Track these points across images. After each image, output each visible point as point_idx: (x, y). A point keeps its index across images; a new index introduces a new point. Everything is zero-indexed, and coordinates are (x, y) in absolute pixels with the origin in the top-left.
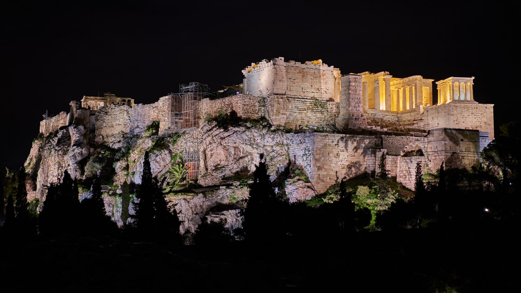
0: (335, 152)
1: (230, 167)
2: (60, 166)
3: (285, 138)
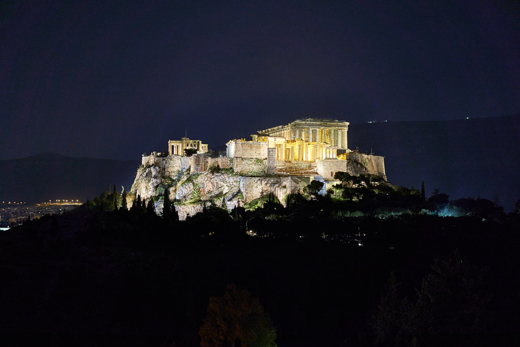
0: (256, 186)
1: (215, 192)
2: (147, 188)
3: (238, 178)
